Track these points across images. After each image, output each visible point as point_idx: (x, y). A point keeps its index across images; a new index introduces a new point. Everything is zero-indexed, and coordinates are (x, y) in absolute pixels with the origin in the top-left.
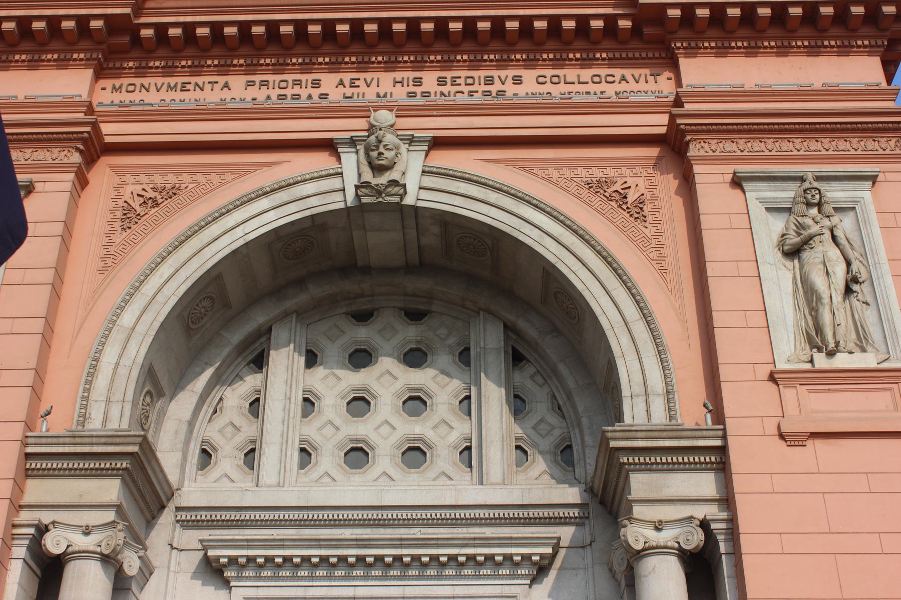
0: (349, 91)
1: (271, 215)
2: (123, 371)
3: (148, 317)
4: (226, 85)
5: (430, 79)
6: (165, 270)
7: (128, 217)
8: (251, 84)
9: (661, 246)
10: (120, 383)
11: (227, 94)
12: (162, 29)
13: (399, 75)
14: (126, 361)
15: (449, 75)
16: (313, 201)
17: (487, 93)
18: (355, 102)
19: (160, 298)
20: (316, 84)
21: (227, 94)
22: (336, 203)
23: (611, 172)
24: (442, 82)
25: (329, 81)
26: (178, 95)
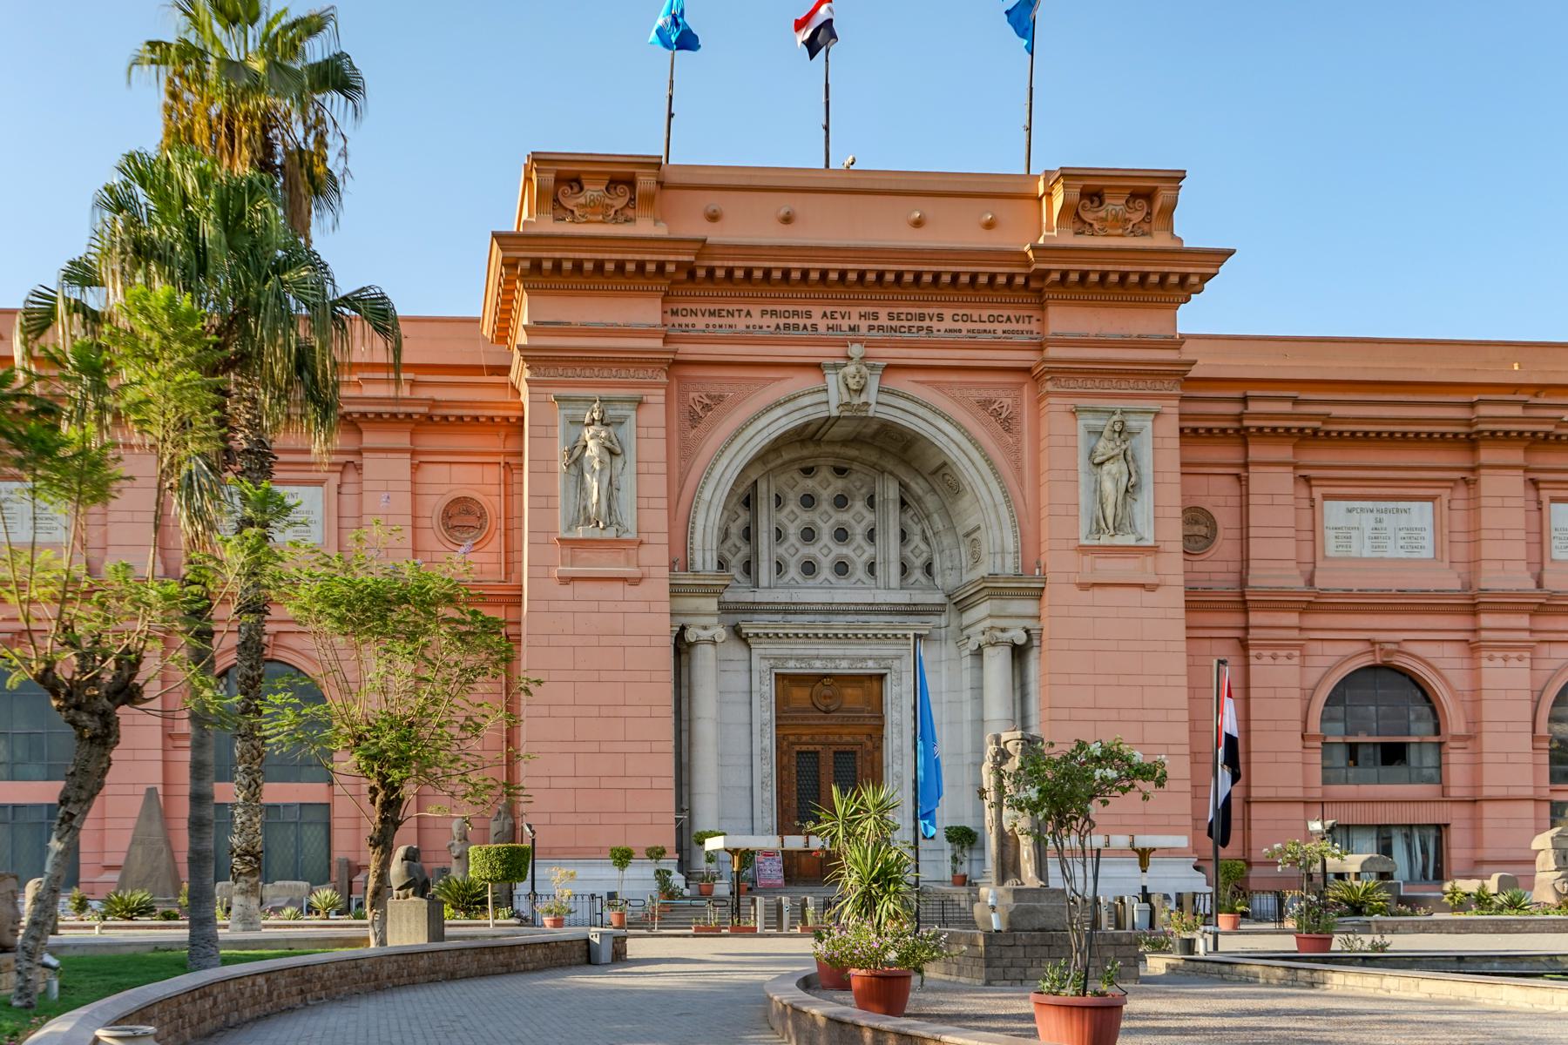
0: (831, 322)
1: (783, 421)
2: (709, 530)
3: (718, 493)
4: (748, 313)
5: (883, 313)
6: (724, 461)
7: (694, 419)
8: (764, 313)
9: (1018, 451)
10: (708, 538)
11: (750, 322)
12: (711, 271)
13: (863, 310)
14: (710, 524)
15: (896, 311)
16: (809, 410)
17: (920, 329)
18: (839, 335)
19: (724, 480)
20: (809, 315)
21: (750, 322)
22: (822, 412)
23: (992, 394)
24: (891, 316)
25: (817, 311)
26: (716, 321)
